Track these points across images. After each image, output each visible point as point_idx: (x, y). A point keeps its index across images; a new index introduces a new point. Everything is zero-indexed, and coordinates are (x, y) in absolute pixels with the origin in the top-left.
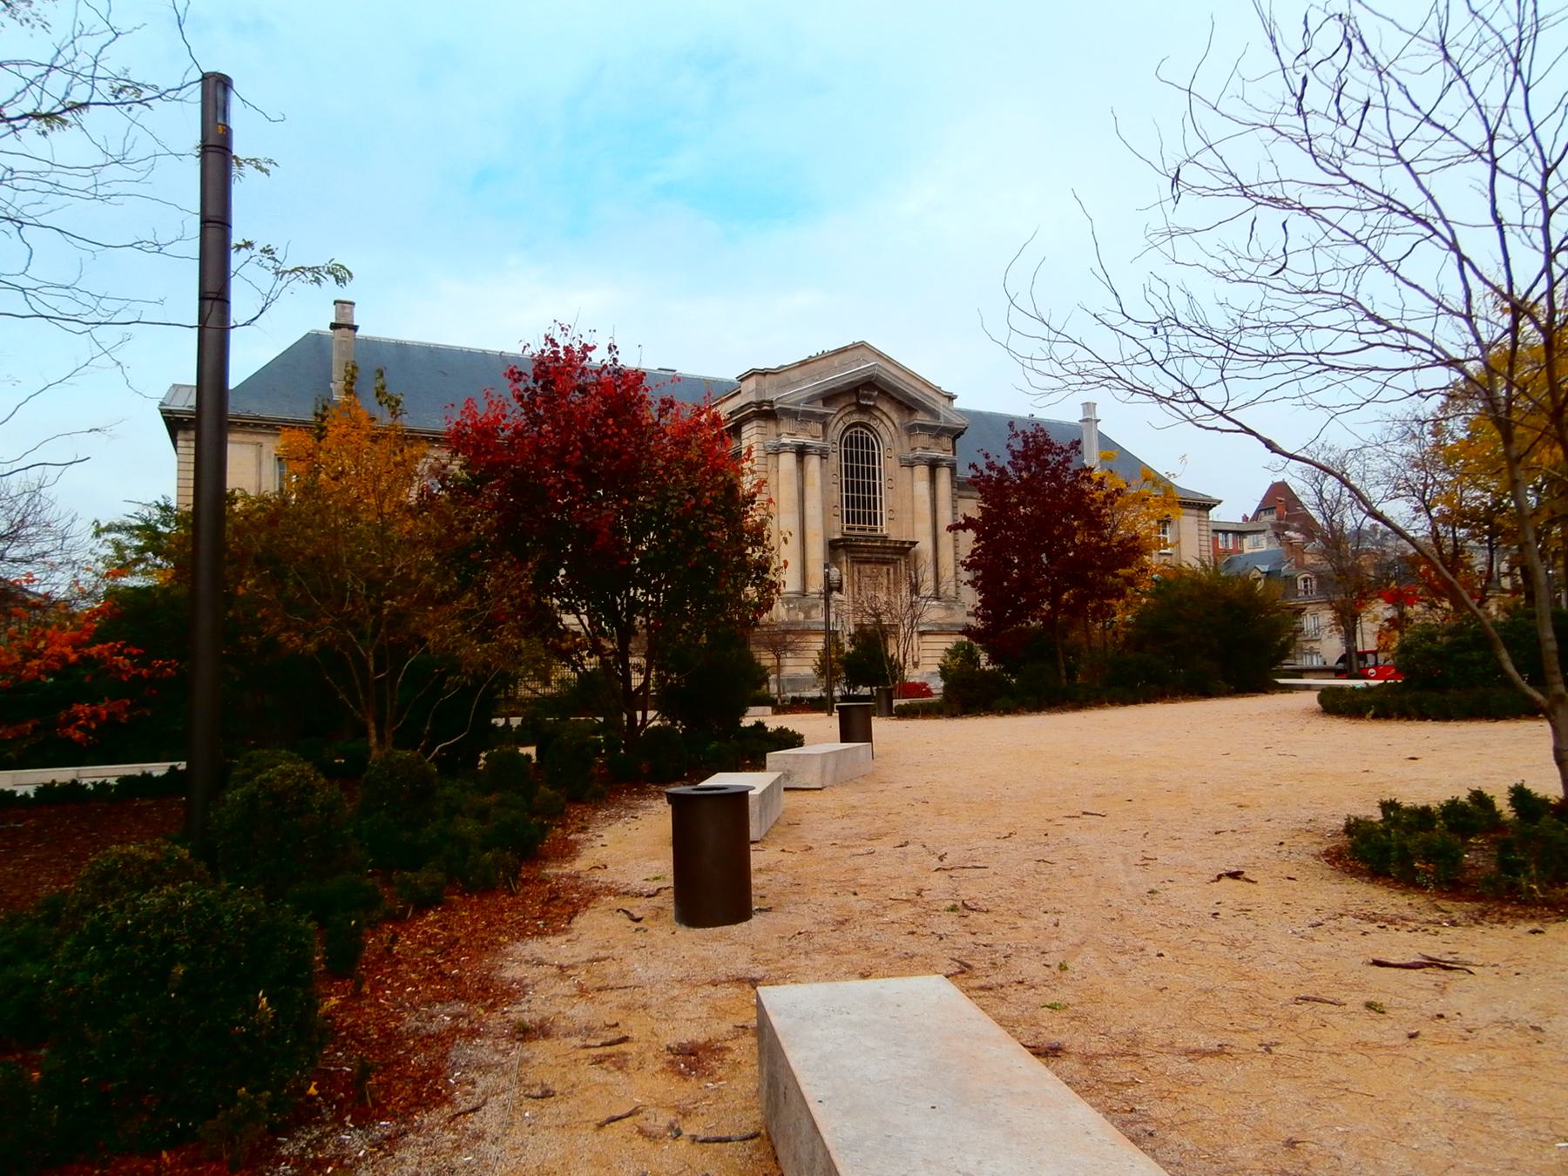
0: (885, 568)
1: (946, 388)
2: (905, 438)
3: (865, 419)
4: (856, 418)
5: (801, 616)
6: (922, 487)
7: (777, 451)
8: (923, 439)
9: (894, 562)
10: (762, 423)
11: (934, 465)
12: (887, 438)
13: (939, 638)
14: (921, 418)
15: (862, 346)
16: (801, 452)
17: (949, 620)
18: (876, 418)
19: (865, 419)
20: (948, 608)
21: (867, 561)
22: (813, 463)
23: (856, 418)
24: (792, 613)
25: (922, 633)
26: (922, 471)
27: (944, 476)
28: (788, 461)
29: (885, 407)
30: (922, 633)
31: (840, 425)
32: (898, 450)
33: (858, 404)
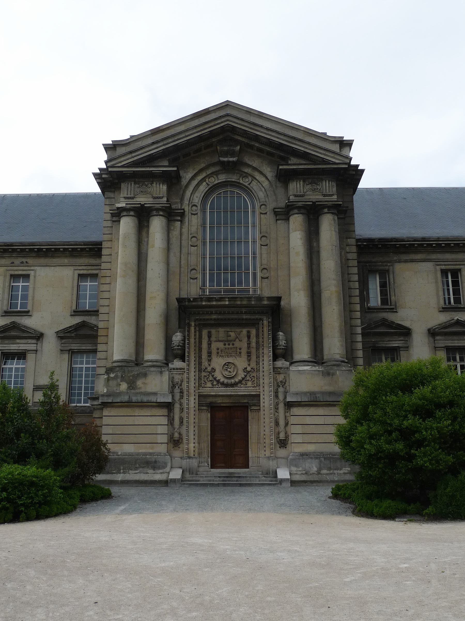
0: (245, 331)
1: (332, 132)
2: (280, 191)
3: (234, 178)
4: (222, 178)
5: (124, 386)
6: (297, 239)
7: (117, 214)
8: (296, 187)
9: (254, 324)
10: (111, 195)
11: (313, 213)
12: (261, 195)
13: (312, 411)
14: (294, 164)
15: (227, 105)
16: (142, 215)
17: (327, 388)
18: (247, 175)
19: (234, 178)
20: (327, 374)
21: (218, 324)
22: (157, 225)
23: (222, 178)
24: (112, 383)
25: (289, 405)
26: (297, 221)
27: (328, 227)
28: (127, 225)
29: (255, 163)
30: (289, 405)
31: (203, 188)
32: (273, 205)
33: (222, 164)
